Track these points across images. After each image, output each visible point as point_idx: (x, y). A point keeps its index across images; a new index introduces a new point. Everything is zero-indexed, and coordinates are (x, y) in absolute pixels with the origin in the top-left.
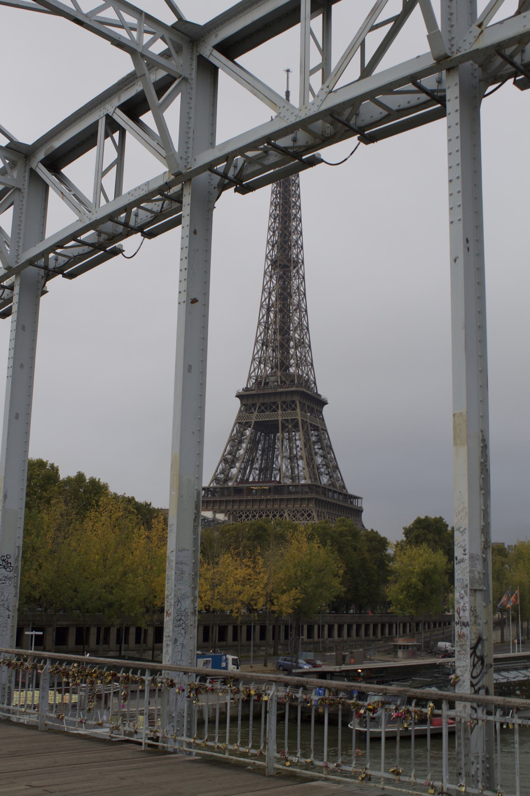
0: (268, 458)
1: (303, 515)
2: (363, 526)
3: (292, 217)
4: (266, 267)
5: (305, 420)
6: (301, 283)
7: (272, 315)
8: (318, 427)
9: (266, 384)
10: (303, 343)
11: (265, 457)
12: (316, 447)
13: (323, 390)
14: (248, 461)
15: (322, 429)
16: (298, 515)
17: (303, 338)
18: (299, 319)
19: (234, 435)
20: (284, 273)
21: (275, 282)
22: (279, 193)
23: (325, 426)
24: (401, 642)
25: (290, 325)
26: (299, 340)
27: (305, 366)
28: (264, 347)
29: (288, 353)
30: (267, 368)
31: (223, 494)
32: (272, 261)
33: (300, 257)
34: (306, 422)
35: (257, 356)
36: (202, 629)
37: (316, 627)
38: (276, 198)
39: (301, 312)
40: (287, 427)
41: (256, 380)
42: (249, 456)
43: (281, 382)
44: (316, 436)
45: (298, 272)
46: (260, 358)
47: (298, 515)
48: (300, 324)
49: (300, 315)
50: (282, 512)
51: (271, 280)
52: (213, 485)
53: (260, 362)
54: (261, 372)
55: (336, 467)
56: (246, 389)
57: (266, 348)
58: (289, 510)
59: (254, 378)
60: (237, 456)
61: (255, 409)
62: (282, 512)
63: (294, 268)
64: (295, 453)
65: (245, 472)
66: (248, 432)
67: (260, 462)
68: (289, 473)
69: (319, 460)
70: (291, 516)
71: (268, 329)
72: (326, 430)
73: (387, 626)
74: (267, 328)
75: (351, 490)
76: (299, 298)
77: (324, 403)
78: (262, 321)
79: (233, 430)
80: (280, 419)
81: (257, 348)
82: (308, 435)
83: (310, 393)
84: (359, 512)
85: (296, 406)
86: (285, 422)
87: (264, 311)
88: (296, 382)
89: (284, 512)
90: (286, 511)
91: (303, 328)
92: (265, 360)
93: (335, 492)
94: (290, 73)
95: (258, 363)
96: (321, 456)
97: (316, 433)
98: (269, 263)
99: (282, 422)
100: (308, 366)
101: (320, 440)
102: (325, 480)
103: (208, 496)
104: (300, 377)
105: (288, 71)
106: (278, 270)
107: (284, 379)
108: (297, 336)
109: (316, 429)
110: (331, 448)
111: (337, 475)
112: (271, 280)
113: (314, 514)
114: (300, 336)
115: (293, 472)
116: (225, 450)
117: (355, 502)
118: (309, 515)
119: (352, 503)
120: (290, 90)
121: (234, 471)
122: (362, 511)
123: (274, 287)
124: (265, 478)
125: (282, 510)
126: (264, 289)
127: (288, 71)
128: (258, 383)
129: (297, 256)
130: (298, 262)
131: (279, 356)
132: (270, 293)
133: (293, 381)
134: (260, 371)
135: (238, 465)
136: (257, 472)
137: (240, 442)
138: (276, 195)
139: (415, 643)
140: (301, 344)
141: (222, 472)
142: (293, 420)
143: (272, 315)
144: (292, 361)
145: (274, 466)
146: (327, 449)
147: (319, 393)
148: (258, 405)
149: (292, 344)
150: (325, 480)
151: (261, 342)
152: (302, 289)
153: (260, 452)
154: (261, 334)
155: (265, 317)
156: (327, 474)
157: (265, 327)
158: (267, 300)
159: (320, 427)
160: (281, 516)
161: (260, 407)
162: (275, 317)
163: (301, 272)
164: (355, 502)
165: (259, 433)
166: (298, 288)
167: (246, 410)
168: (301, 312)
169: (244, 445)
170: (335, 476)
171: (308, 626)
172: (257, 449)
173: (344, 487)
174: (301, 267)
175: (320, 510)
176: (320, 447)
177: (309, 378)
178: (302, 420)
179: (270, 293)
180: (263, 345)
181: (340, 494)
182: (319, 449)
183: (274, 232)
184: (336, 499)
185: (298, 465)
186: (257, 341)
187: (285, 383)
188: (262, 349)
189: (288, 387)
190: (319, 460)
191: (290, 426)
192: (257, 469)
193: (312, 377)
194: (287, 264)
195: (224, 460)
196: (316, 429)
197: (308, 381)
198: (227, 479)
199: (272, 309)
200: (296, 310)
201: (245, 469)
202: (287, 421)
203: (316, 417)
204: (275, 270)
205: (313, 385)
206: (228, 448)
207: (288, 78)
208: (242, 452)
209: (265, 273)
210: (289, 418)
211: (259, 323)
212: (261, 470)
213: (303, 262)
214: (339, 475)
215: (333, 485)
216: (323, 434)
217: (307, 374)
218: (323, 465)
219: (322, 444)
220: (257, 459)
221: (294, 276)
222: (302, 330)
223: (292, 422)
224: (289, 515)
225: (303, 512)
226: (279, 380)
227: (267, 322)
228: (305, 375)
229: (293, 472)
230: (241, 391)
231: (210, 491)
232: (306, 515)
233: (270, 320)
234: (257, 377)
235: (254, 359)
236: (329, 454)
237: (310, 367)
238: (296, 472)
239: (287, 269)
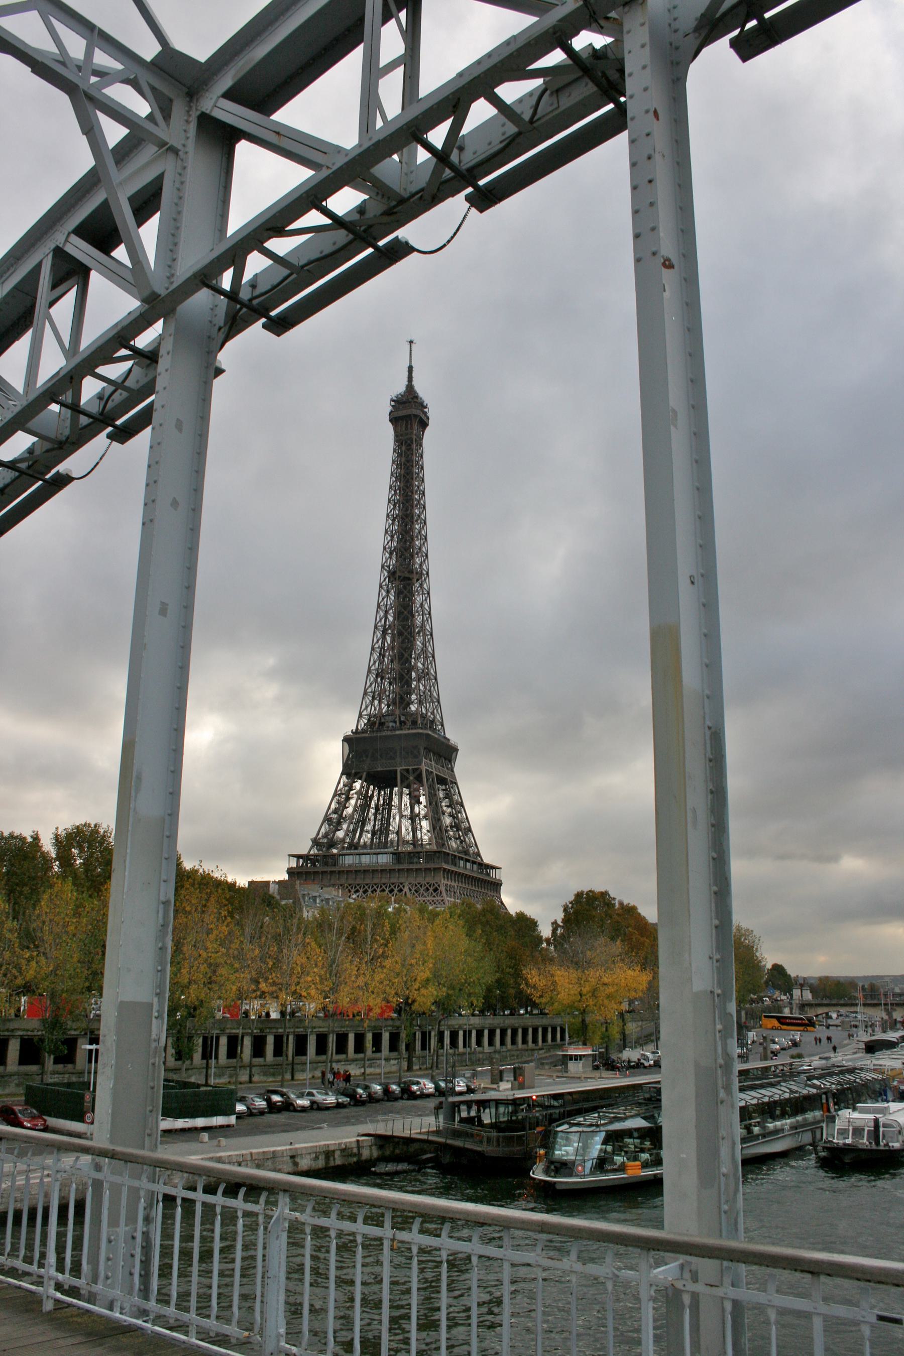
0: (382, 818)
1: (428, 889)
3: (415, 518)
4: (382, 579)
5: (430, 770)
6: (426, 600)
7: (389, 639)
8: (447, 779)
9: (382, 724)
10: (428, 674)
11: (380, 817)
12: (443, 804)
14: (358, 822)
15: (452, 782)
16: (422, 890)
17: (428, 668)
18: (423, 644)
19: (341, 790)
20: (405, 587)
21: (393, 598)
22: (399, 489)
23: (455, 779)
24: (572, 1052)
25: (411, 652)
26: (423, 671)
27: (430, 703)
28: (379, 679)
29: (409, 685)
30: (383, 705)
31: (326, 864)
32: (389, 572)
33: (424, 567)
34: (432, 772)
35: (369, 690)
36: (315, 1038)
37: (461, 1033)
38: (395, 494)
39: (425, 635)
40: (408, 779)
41: (369, 720)
43: (401, 722)
44: (443, 790)
45: (421, 585)
46: (374, 692)
47: (422, 890)
48: (424, 650)
49: (424, 639)
50: (401, 886)
51: (387, 596)
52: (314, 851)
53: (374, 698)
54: (375, 709)
55: (469, 829)
56: (356, 732)
57: (381, 680)
58: (410, 884)
59: (367, 717)
60: (344, 816)
61: (367, 756)
62: (401, 886)
63: (417, 580)
64: (417, 812)
66: (357, 785)
67: (372, 823)
68: (410, 837)
69: (447, 820)
70: (413, 891)
71: (384, 656)
72: (456, 783)
73: (550, 1030)
74: (382, 655)
75: (487, 859)
76: (423, 617)
78: (376, 646)
79: (339, 783)
81: (370, 680)
82: (434, 789)
83: (436, 736)
84: (496, 886)
85: (419, 752)
86: (405, 773)
87: (379, 634)
88: (419, 722)
89: (404, 887)
90: (406, 884)
91: (429, 656)
92: (379, 695)
93: (467, 861)
94: (413, 345)
95: (371, 698)
96: (450, 816)
98: (386, 574)
99: (401, 773)
100: (433, 702)
101: (448, 796)
103: (307, 865)
104: (424, 717)
105: (411, 342)
106: (398, 582)
107: (403, 718)
108: (419, 665)
109: (442, 781)
111: (469, 839)
112: (387, 596)
113: (443, 888)
114: (423, 665)
115: (414, 835)
116: (329, 808)
117: (492, 873)
118: (436, 890)
119: (488, 874)
120: (413, 364)
121: (340, 834)
122: (501, 885)
123: (391, 604)
125: (401, 884)
126: (379, 606)
127: (411, 342)
128: (370, 723)
129: (421, 565)
130: (421, 574)
131: (398, 690)
132: (386, 612)
133: (414, 723)
134: (373, 708)
135: (345, 826)
136: (369, 836)
137: (348, 799)
138: (395, 491)
139: (590, 1052)
140: (425, 675)
141: (326, 835)
142: (415, 770)
143: (389, 639)
144: (414, 697)
145: (391, 828)
147: (447, 736)
149: (413, 674)
151: (375, 672)
152: (426, 606)
154: (375, 662)
155: (380, 641)
157: (380, 653)
158: (383, 620)
159: (449, 779)
160: (401, 890)
162: (393, 641)
163: (425, 586)
164: (492, 873)
165: (371, 787)
166: (422, 605)
168: (425, 635)
169: (353, 802)
170: (467, 840)
171: (451, 1032)
172: (369, 806)
173: (478, 854)
174: (425, 580)
175: (449, 883)
176: (448, 804)
177: (435, 717)
178: (427, 770)
179: (386, 612)
180: (377, 676)
181: (474, 863)
183: (392, 536)
184: (467, 868)
185: (421, 826)
186: (369, 671)
187: (405, 723)
188: (376, 681)
189: (409, 729)
190: (447, 820)
191: (411, 778)
192: (368, 832)
193: (438, 717)
194: (407, 575)
195: (327, 819)
196: (442, 781)
197: (432, 722)
198: (332, 844)
199: (390, 631)
200: (419, 633)
201: (355, 831)
202: (407, 770)
203: (443, 767)
204: (392, 584)
205: (440, 727)
206: (333, 806)
207: (411, 350)
208: (350, 810)
209: (381, 586)
210: (410, 768)
211: (373, 649)
212: (374, 833)
213: (428, 574)
216: (452, 787)
217: (433, 713)
219: (451, 800)
220: (369, 819)
221: (417, 591)
222: (426, 658)
223: (414, 772)
224: (410, 890)
225: (427, 886)
226: (397, 720)
227: (382, 648)
228: (429, 714)
229: (414, 835)
230: (350, 733)
231: (310, 859)
232: (431, 890)
233: (386, 645)
234: (370, 716)
235: (365, 693)
237: (436, 703)
238: (419, 836)
239: (408, 582)
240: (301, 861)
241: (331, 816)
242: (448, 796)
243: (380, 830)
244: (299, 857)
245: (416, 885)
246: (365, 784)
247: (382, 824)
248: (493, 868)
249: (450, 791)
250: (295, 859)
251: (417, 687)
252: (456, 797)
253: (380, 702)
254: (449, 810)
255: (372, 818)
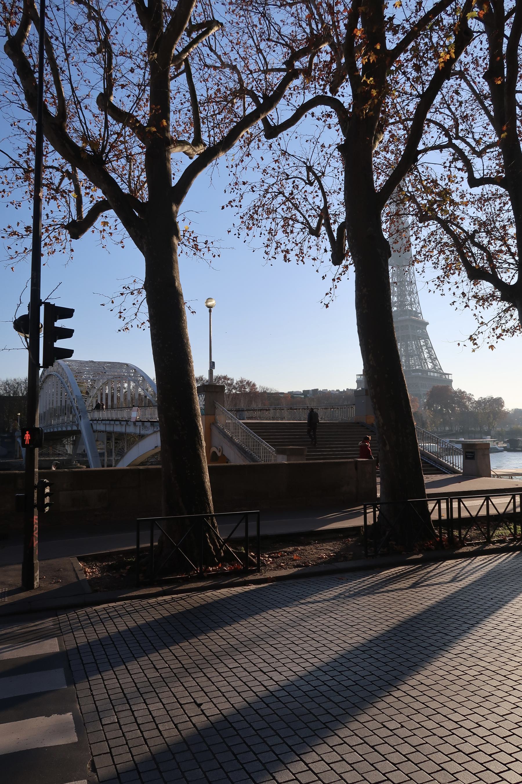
10: (413, 292)
13: (426, 317)
55: (436, 358)
75: (445, 372)
77: (428, 324)
97: (423, 341)
101: (426, 345)
102: (430, 366)
110: (432, 348)
140: (411, 293)
146: (430, 349)
150: (430, 366)
173: (441, 369)
215: (434, 368)
242: (426, 345)
248: (448, 374)
252: (429, 345)
254: (426, 350)
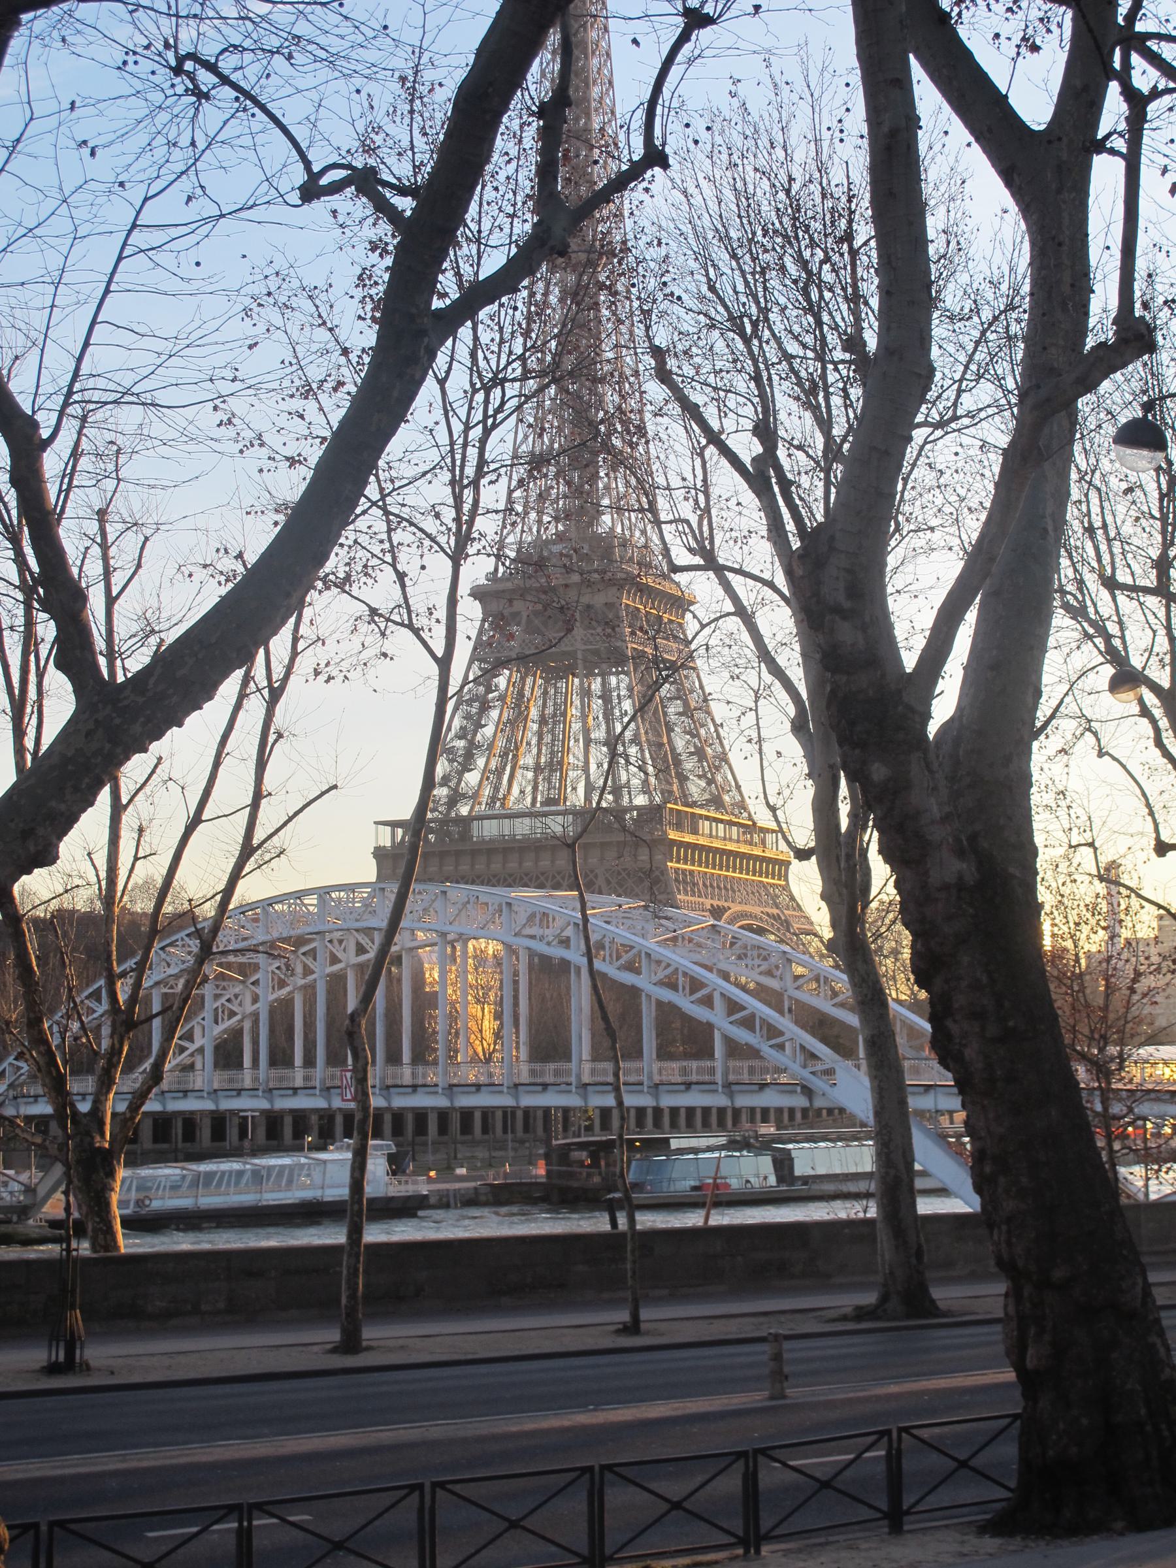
0: (553, 740)
2: (792, 898)
11: (548, 738)
30: (546, 519)
41: (519, 551)
42: (509, 740)
50: (591, 876)
65: (500, 778)
66: (501, 682)
67: (535, 751)
80: (580, 646)
89: (596, 876)
121: (472, 778)
124: (549, 789)
125: (592, 871)
135: (481, 762)
136: (530, 775)
137: (485, 707)
148: (524, 615)
153: (535, 727)
156: (699, 777)
161: (529, 621)
165: (529, 680)
167: (495, 626)
169: (494, 714)
170: (719, 778)
182: (680, 714)
190: (680, 742)
201: (499, 772)
208: (489, 731)
212: (537, 769)
214: (730, 777)
216: (686, 677)
218: (691, 754)
219: (686, 704)
220: (529, 744)
230: (483, 581)
236: (702, 726)
240: (400, 832)
241: (454, 744)
243: (550, 764)
244: (394, 825)
245: (619, 874)
246: (516, 676)
247: (552, 753)
249: (682, 684)
250: (389, 828)
251: (607, 488)
253: (540, 513)
255: (534, 741)
